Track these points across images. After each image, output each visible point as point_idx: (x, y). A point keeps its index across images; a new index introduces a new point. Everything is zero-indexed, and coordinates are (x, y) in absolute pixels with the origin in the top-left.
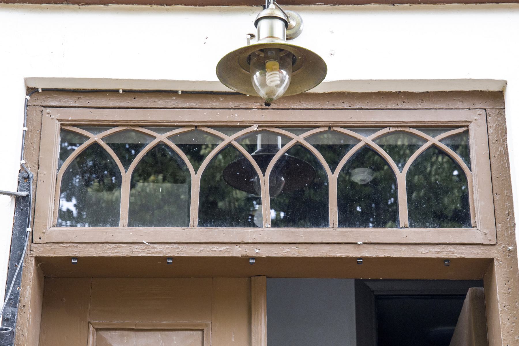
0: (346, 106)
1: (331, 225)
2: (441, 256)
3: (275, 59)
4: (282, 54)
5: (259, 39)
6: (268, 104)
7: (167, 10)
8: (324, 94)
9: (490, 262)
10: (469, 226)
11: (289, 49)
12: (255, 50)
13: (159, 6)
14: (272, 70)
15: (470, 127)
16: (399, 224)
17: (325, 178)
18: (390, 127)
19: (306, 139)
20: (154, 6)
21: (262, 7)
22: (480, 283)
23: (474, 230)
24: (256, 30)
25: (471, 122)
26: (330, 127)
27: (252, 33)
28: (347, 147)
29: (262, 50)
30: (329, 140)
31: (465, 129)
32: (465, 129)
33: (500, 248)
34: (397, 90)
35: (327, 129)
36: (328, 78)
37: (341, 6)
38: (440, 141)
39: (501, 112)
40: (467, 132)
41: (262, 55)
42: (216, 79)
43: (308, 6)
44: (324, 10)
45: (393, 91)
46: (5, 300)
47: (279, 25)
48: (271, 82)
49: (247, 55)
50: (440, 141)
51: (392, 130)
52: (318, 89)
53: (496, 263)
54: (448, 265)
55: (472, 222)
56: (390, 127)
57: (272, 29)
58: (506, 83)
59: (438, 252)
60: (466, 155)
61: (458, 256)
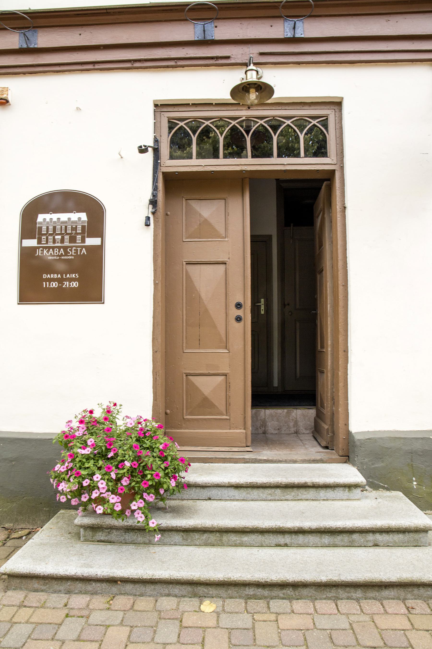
0: (280, 108)
1: (274, 157)
2: (316, 169)
3: (253, 88)
4: (256, 86)
5: (247, 79)
6: (249, 108)
7: (208, 69)
8: (271, 103)
9: (334, 171)
10: (327, 157)
11: (259, 83)
12: (245, 84)
13: (205, 67)
14: (253, 93)
15: (328, 117)
16: (300, 156)
17: (272, 138)
18: (297, 117)
19: (264, 122)
20: (203, 67)
21: (246, 67)
22: (329, 180)
23: (329, 158)
24: (245, 75)
25: (329, 115)
26: (274, 117)
27: (243, 78)
28: (280, 126)
29: (248, 84)
30: (274, 123)
31: (327, 117)
32: (327, 117)
33: (338, 165)
34: (300, 101)
35: (272, 118)
36: (275, 96)
37: (278, 65)
38: (317, 122)
39: (341, 110)
40: (327, 119)
41: (248, 86)
42: (230, 98)
43: (265, 66)
44: (271, 67)
45: (299, 102)
46: (168, 137)
47: (254, 73)
48: (252, 98)
49: (242, 86)
50: (317, 122)
51: (298, 118)
52: (269, 101)
53: (336, 171)
54: (318, 172)
55: (328, 155)
56: (297, 117)
57: (252, 74)
58: (342, 98)
59: (315, 167)
60: (326, 128)
61: (323, 169)
